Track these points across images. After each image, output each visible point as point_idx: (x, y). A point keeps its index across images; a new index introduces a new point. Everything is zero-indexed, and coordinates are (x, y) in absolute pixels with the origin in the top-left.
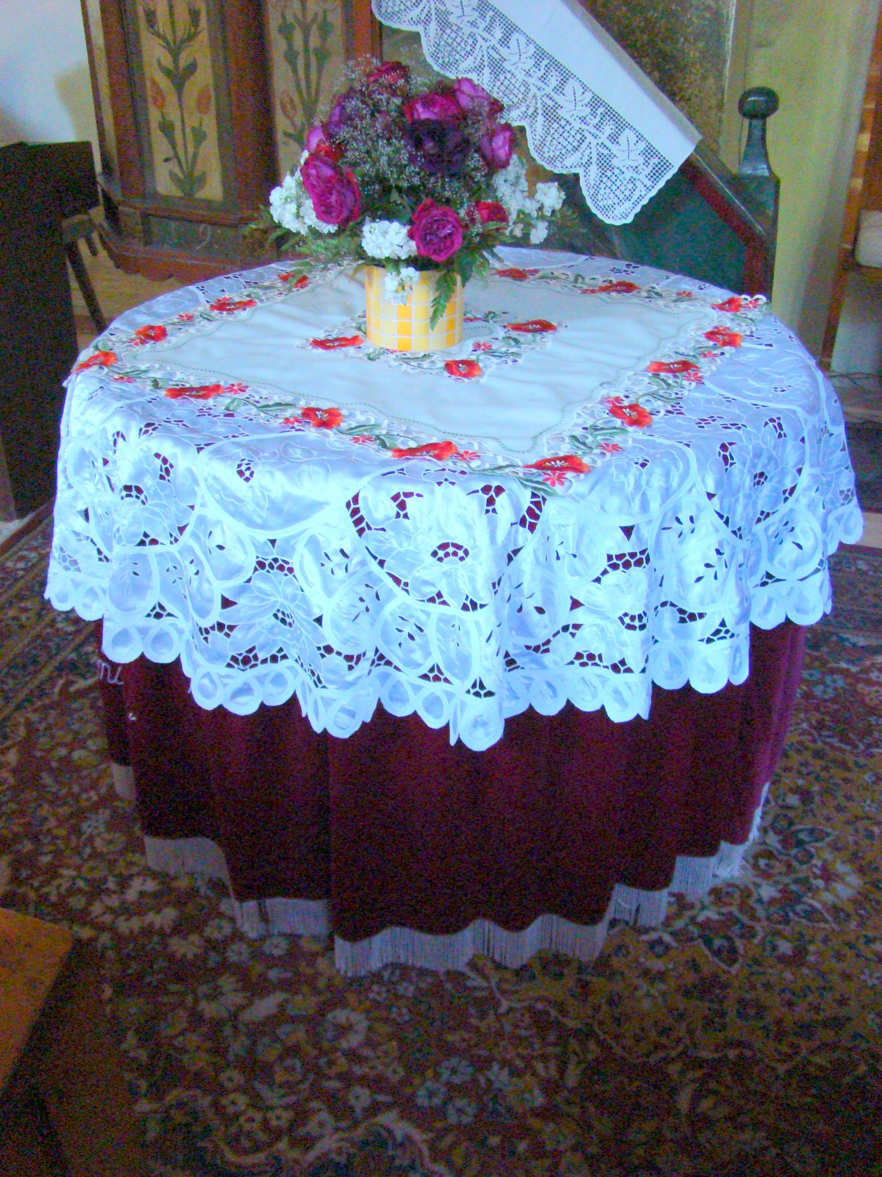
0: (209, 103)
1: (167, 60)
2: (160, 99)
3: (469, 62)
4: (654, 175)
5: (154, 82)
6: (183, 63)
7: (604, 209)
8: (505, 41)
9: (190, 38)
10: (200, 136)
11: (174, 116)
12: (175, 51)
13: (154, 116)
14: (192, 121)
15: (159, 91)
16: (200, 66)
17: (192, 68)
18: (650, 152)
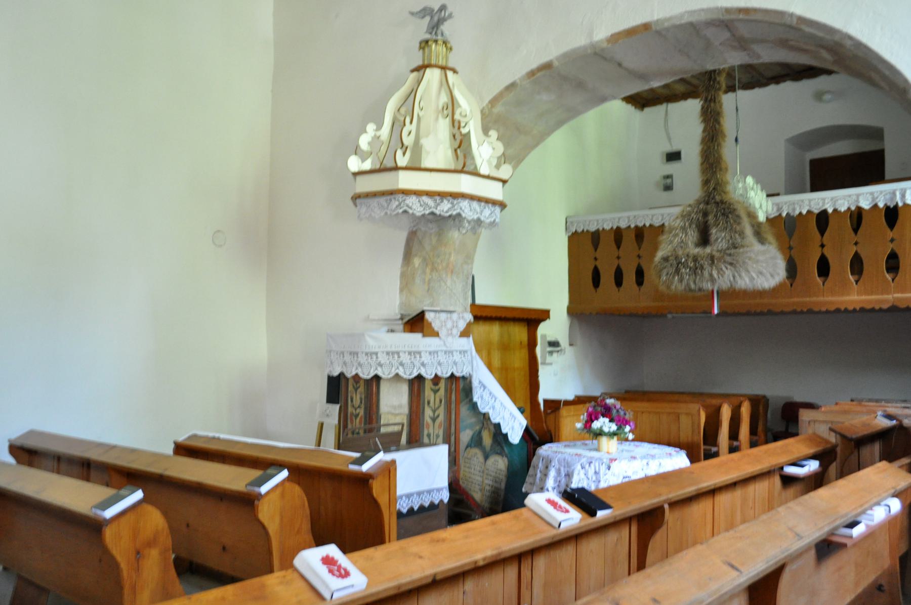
0: (441, 426)
1: (431, 414)
2: (428, 428)
3: (488, 407)
4: (522, 429)
5: (427, 421)
6: (436, 415)
7: (513, 440)
8: (495, 401)
9: (439, 407)
10: (438, 436)
11: (431, 431)
12: (434, 411)
13: (426, 432)
14: (436, 432)
15: (428, 424)
16: (440, 416)
17: (438, 416)
18: (520, 424)
